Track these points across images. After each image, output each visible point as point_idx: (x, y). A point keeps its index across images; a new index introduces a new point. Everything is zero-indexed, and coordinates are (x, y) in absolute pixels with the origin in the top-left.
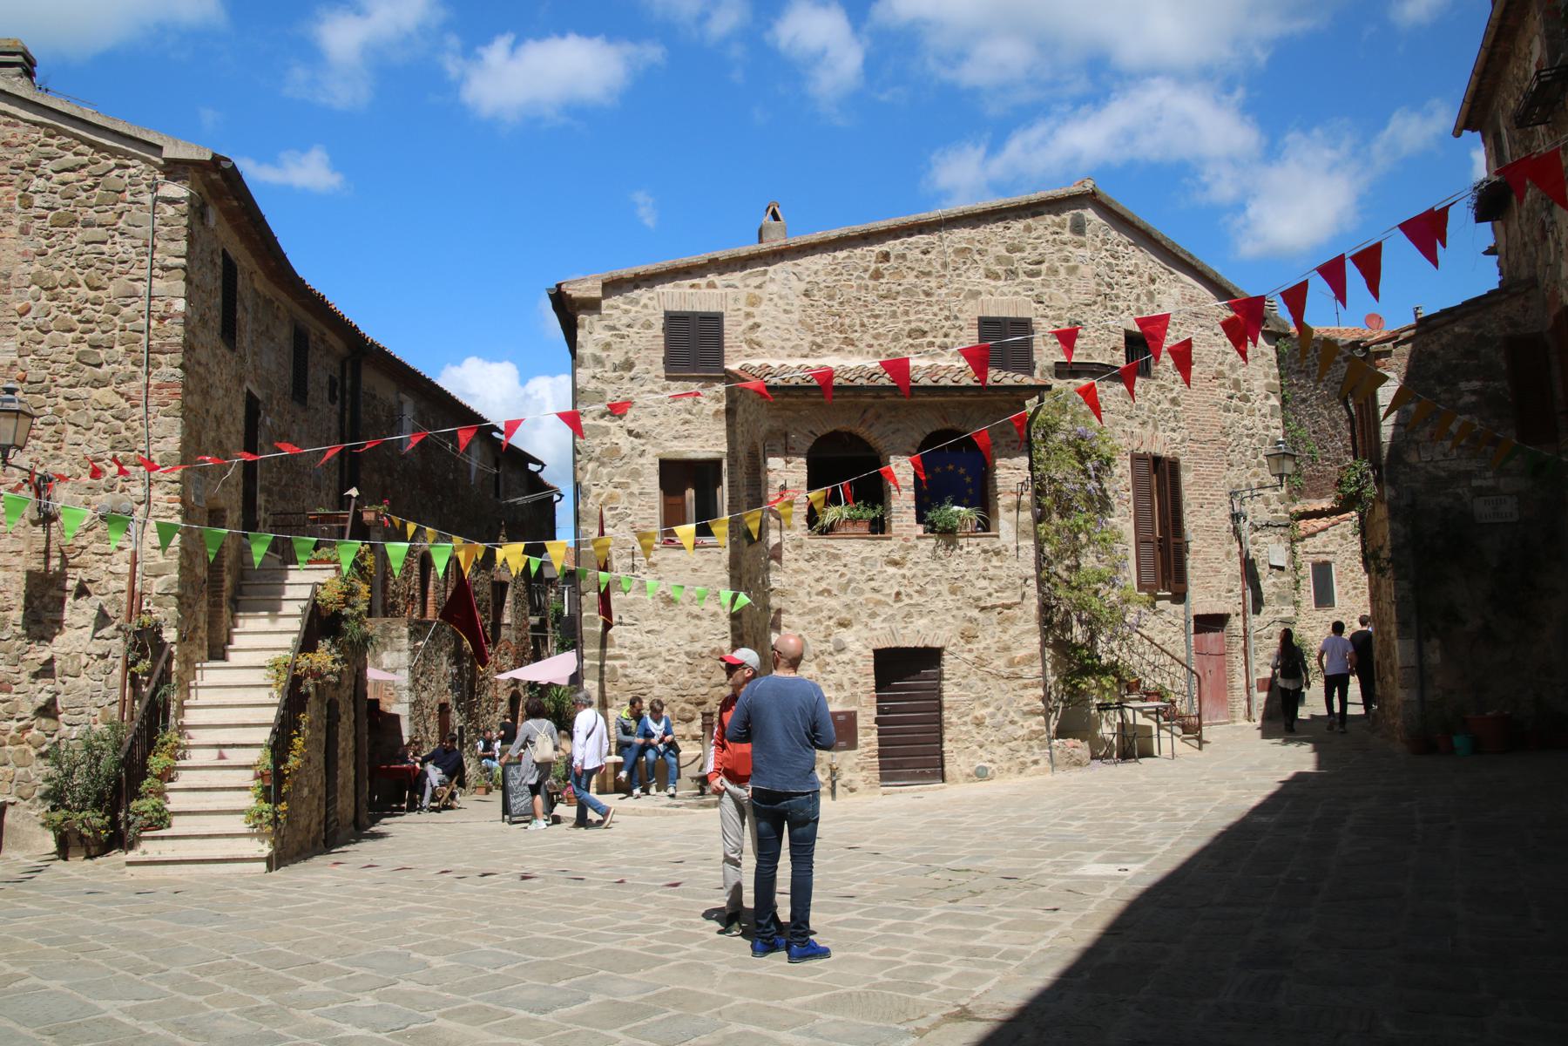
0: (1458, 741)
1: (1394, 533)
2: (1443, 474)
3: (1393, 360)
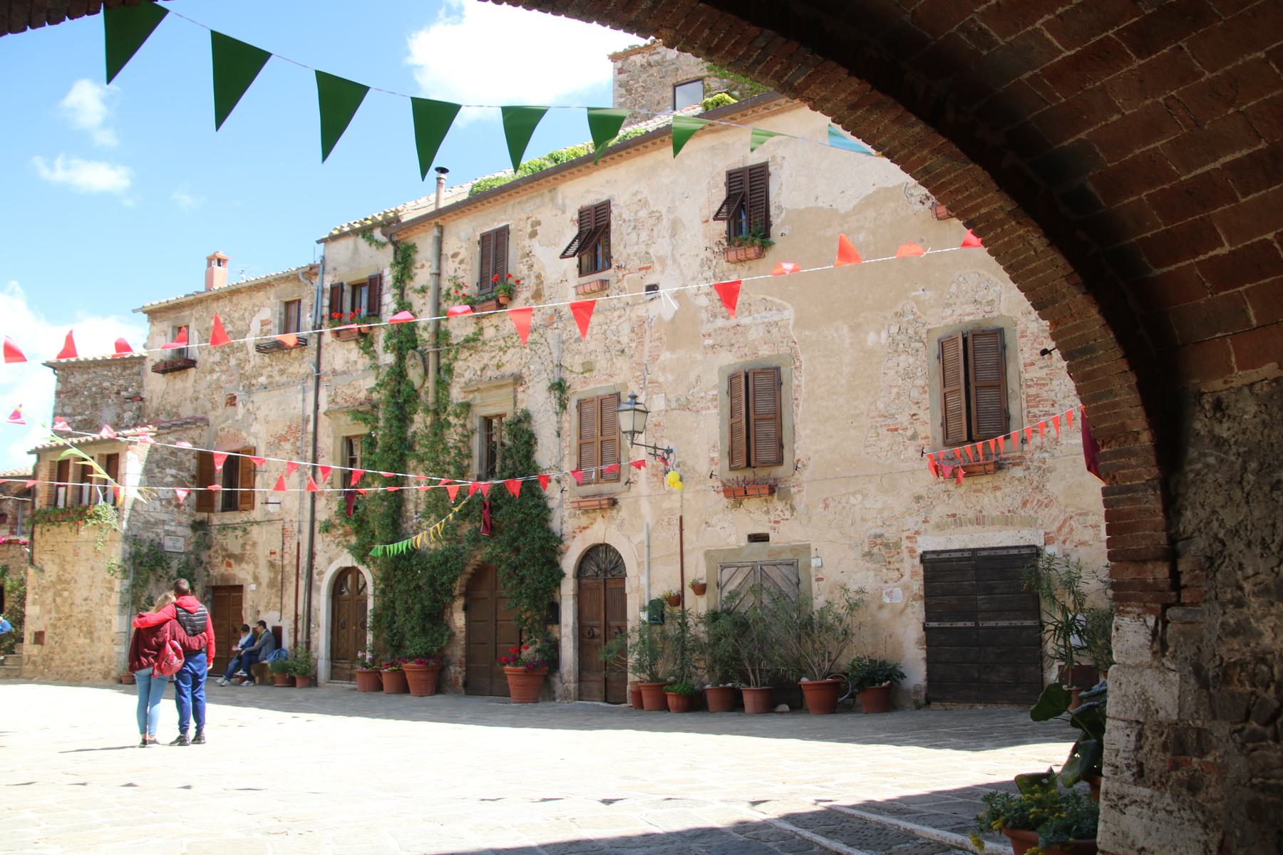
1: (124, 552)
2: (152, 520)
3: (136, 447)
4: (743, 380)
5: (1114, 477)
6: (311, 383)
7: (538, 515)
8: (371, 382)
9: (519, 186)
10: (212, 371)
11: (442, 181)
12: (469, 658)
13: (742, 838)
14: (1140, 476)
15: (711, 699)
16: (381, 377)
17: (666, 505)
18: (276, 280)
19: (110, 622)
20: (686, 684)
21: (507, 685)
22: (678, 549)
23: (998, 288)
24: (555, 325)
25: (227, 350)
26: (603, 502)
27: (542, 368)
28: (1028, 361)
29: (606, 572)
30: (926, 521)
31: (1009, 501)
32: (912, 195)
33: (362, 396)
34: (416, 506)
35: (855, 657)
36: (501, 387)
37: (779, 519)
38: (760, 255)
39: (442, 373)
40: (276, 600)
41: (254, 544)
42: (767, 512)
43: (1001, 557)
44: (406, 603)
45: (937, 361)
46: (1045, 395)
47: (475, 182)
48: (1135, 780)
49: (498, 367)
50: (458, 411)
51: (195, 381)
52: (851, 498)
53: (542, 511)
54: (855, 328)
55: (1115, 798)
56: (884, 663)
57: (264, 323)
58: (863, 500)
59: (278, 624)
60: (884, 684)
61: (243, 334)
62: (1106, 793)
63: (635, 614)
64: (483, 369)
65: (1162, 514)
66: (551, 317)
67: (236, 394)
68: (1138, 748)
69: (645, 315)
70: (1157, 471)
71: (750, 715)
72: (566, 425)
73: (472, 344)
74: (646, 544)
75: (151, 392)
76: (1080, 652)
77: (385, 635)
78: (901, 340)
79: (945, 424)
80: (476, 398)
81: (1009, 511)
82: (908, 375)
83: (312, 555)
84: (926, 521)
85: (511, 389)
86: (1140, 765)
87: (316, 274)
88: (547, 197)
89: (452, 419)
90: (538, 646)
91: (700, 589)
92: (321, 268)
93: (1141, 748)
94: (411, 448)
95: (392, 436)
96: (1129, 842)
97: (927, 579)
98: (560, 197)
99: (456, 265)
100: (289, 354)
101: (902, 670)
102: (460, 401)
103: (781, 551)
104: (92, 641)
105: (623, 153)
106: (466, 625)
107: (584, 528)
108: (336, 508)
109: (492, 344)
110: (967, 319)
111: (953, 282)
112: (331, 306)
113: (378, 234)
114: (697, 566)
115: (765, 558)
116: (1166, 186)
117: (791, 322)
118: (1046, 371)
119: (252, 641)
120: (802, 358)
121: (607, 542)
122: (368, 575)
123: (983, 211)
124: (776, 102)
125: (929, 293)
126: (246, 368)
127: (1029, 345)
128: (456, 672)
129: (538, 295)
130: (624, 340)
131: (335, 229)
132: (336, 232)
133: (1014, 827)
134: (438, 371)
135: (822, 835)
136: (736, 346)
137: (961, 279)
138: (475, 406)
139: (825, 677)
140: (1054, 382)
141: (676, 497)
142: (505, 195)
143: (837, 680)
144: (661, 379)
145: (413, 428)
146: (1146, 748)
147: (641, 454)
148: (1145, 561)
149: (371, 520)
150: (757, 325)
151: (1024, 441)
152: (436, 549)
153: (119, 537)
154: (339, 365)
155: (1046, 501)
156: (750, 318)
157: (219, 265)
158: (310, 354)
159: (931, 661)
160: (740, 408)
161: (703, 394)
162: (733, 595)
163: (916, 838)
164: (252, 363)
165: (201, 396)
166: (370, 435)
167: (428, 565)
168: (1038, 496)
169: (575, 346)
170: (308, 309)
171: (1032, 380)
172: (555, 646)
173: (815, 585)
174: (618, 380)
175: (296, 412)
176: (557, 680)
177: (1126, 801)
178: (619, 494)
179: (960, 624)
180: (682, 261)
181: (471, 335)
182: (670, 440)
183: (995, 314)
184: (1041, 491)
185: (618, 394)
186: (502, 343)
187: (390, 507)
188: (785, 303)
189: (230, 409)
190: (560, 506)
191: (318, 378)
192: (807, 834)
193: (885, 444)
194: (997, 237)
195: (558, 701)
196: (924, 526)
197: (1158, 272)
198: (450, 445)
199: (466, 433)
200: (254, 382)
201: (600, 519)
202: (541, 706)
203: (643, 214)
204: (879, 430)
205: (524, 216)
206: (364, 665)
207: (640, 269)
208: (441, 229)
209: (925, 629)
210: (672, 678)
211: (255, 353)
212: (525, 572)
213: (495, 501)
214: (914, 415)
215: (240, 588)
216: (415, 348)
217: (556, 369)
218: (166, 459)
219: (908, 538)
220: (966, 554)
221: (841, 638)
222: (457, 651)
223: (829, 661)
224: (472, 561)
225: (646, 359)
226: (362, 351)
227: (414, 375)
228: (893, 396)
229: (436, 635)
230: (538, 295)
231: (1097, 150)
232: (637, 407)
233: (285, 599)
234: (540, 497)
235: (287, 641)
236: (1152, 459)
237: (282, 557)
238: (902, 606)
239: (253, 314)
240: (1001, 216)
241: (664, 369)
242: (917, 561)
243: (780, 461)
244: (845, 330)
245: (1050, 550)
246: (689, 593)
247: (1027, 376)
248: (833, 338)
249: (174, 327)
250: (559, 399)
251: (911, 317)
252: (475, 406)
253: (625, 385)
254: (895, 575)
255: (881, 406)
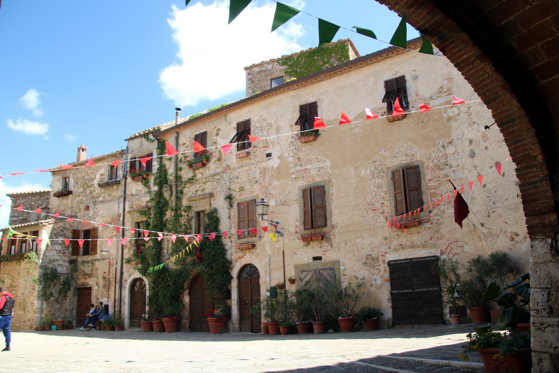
0: (54, 327)
1: (40, 273)
2: (52, 259)
4: (309, 191)
5: (525, 179)
6: (122, 200)
7: (221, 252)
8: (148, 198)
9: (212, 114)
10: (79, 196)
11: (178, 114)
12: (191, 316)
13: (343, 369)
14: (538, 176)
15: (299, 328)
16: (152, 196)
17: (277, 246)
18: (107, 156)
19: (33, 303)
20: (288, 322)
21: (209, 327)
22: (283, 265)
23: (416, 149)
24: (227, 172)
25: (86, 187)
26: (249, 246)
27: (222, 190)
28: (430, 179)
29: (251, 276)
30: (389, 248)
31: (425, 238)
32: (378, 113)
33: (144, 204)
34: (168, 250)
35: (362, 307)
36: (204, 198)
37: (326, 250)
38: (315, 139)
39: (179, 193)
40: (106, 293)
41: (97, 269)
42: (321, 247)
43: (422, 261)
44: (163, 292)
45: (391, 180)
46: (437, 192)
47: (191, 116)
48: (549, 315)
49: (203, 190)
50: (186, 209)
51: (72, 200)
52: (357, 240)
53: (222, 251)
54: (356, 168)
55: (539, 325)
56: (374, 310)
57: (102, 175)
58: (362, 240)
59: (107, 304)
60: (375, 318)
61: (93, 180)
62: (534, 323)
63: (264, 293)
64: (196, 191)
65: (551, 191)
66: (226, 168)
67: (89, 205)
68: (549, 300)
69: (266, 166)
70: (547, 172)
71: (316, 334)
72: (233, 214)
73: (192, 181)
74: (268, 263)
75: (53, 205)
76: (459, 300)
77: (154, 307)
78: (376, 172)
79: (396, 206)
80: (194, 204)
81: (425, 242)
82: (379, 187)
83: (122, 273)
84: (389, 248)
85: (209, 199)
86: (551, 308)
87: (124, 154)
88: (223, 119)
89: (183, 213)
90: (222, 309)
91: (292, 281)
92: (126, 151)
93: (550, 300)
94: (165, 225)
95: (157, 221)
96: (549, 344)
97: (391, 273)
98: (229, 118)
99: (184, 148)
100: (112, 187)
101: (382, 312)
102: (187, 205)
103: (327, 263)
104: (25, 312)
105: (256, 99)
106: (190, 301)
107: (241, 257)
108: (133, 253)
109: (200, 181)
110: (403, 162)
111: (397, 148)
112: (131, 167)
113: (151, 136)
114: (291, 272)
115: (320, 267)
116: (550, 39)
117: (329, 167)
118: (437, 182)
119: (95, 311)
120: (334, 181)
121: (251, 263)
122: (146, 281)
123: (465, 57)
124: (320, 76)
125: (387, 153)
126: (94, 194)
127: (430, 172)
128: (185, 322)
129: (219, 159)
130: (257, 177)
131: (133, 135)
132: (133, 136)
133: (484, 347)
134: (177, 193)
135: (380, 366)
136: (305, 177)
137: (400, 146)
138: (193, 207)
139: (349, 317)
140: (441, 187)
141: (281, 242)
142: (205, 118)
143: (354, 317)
144: (274, 193)
145: (166, 217)
146: (553, 300)
147: (266, 224)
148: (543, 214)
149: (147, 257)
150: (314, 168)
151: (430, 212)
152: (176, 269)
153: (38, 266)
154: (134, 192)
155: (440, 237)
156: (311, 166)
157: (83, 151)
158: (122, 187)
159: (394, 307)
160: (308, 203)
161: (292, 198)
162: (307, 283)
163: (425, 364)
164: (97, 192)
165: (74, 206)
166: (147, 221)
167: (173, 276)
168: (437, 235)
169: (236, 180)
170: (121, 168)
171: (432, 186)
172: (229, 309)
173: (342, 277)
174: (255, 194)
175: (115, 212)
176: (230, 323)
177: (545, 326)
178: (256, 242)
179: (406, 291)
180: (282, 143)
181: (191, 177)
182: (278, 218)
183: (415, 160)
184: (438, 233)
185: (255, 200)
186: (204, 180)
187: (156, 251)
188: (326, 159)
189: (87, 212)
190: (230, 248)
191: (125, 197)
192: (373, 366)
193: (370, 216)
194: (470, 70)
195: (231, 332)
196: (389, 250)
197: (542, 82)
198: (182, 224)
199: (189, 219)
200: (97, 200)
201: (248, 253)
202: (223, 335)
203: (264, 124)
204: (368, 210)
205: (213, 127)
206: (145, 320)
207: (263, 147)
208: (178, 133)
209: (391, 294)
210: (281, 320)
211: (98, 187)
212: (216, 277)
213: (202, 247)
214: (383, 203)
215: (90, 289)
216: (167, 183)
217: (228, 190)
218: (59, 233)
219: (382, 255)
220: (407, 261)
221: (355, 299)
222: (186, 313)
223: (350, 310)
224: (192, 274)
225: (267, 184)
226: (144, 186)
227: (166, 195)
228: (373, 196)
229: (177, 306)
230: (219, 159)
231: (518, 25)
232: (264, 204)
233: (110, 293)
234: (222, 245)
235: (111, 311)
236: (544, 167)
237: (109, 274)
238: (381, 284)
239: (97, 171)
240: (473, 58)
241: (274, 189)
242: (386, 265)
243: (326, 225)
244: (352, 169)
245: (443, 257)
246: (288, 283)
247: (430, 185)
248: (347, 173)
249: (63, 178)
250: (229, 203)
251: (380, 163)
252: (193, 207)
253: (258, 196)
254: (377, 271)
255: (368, 200)
